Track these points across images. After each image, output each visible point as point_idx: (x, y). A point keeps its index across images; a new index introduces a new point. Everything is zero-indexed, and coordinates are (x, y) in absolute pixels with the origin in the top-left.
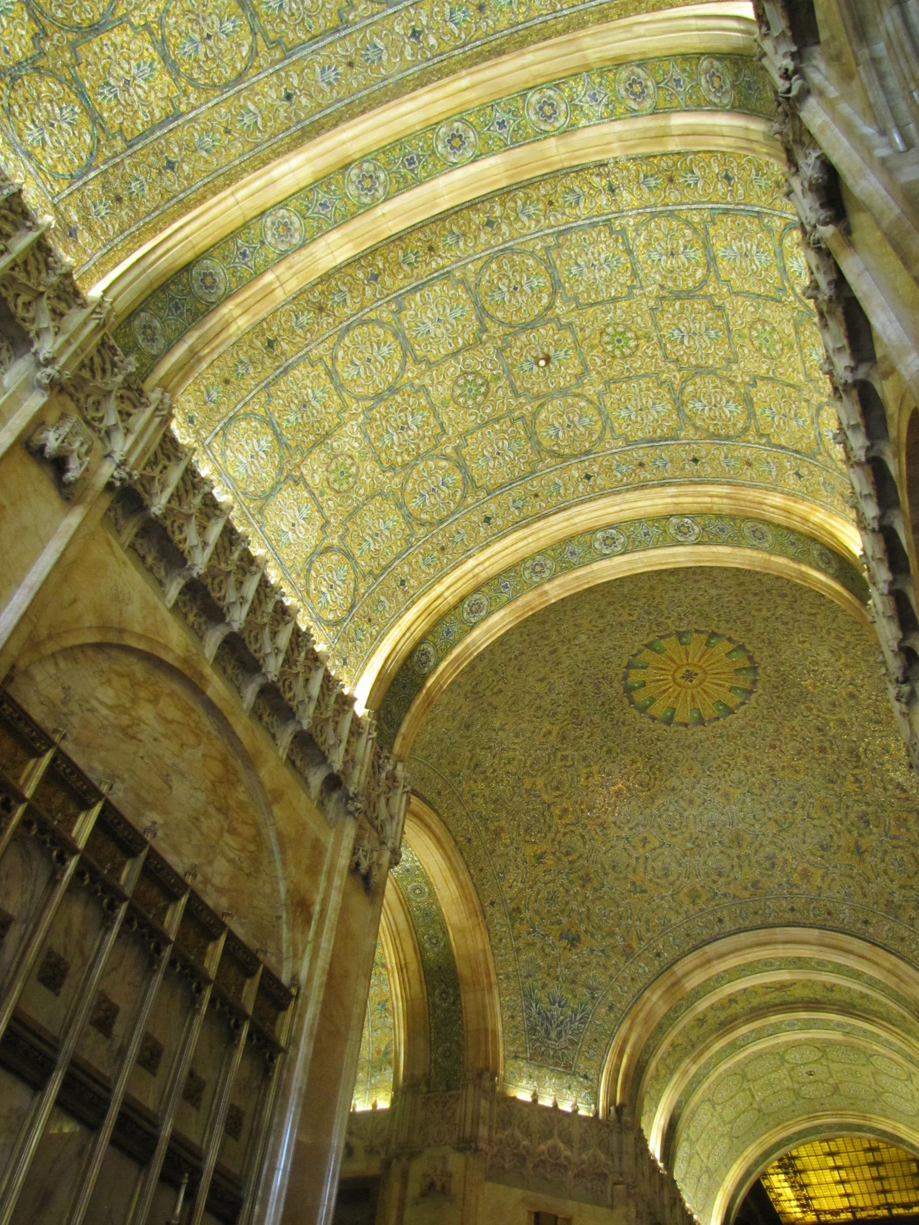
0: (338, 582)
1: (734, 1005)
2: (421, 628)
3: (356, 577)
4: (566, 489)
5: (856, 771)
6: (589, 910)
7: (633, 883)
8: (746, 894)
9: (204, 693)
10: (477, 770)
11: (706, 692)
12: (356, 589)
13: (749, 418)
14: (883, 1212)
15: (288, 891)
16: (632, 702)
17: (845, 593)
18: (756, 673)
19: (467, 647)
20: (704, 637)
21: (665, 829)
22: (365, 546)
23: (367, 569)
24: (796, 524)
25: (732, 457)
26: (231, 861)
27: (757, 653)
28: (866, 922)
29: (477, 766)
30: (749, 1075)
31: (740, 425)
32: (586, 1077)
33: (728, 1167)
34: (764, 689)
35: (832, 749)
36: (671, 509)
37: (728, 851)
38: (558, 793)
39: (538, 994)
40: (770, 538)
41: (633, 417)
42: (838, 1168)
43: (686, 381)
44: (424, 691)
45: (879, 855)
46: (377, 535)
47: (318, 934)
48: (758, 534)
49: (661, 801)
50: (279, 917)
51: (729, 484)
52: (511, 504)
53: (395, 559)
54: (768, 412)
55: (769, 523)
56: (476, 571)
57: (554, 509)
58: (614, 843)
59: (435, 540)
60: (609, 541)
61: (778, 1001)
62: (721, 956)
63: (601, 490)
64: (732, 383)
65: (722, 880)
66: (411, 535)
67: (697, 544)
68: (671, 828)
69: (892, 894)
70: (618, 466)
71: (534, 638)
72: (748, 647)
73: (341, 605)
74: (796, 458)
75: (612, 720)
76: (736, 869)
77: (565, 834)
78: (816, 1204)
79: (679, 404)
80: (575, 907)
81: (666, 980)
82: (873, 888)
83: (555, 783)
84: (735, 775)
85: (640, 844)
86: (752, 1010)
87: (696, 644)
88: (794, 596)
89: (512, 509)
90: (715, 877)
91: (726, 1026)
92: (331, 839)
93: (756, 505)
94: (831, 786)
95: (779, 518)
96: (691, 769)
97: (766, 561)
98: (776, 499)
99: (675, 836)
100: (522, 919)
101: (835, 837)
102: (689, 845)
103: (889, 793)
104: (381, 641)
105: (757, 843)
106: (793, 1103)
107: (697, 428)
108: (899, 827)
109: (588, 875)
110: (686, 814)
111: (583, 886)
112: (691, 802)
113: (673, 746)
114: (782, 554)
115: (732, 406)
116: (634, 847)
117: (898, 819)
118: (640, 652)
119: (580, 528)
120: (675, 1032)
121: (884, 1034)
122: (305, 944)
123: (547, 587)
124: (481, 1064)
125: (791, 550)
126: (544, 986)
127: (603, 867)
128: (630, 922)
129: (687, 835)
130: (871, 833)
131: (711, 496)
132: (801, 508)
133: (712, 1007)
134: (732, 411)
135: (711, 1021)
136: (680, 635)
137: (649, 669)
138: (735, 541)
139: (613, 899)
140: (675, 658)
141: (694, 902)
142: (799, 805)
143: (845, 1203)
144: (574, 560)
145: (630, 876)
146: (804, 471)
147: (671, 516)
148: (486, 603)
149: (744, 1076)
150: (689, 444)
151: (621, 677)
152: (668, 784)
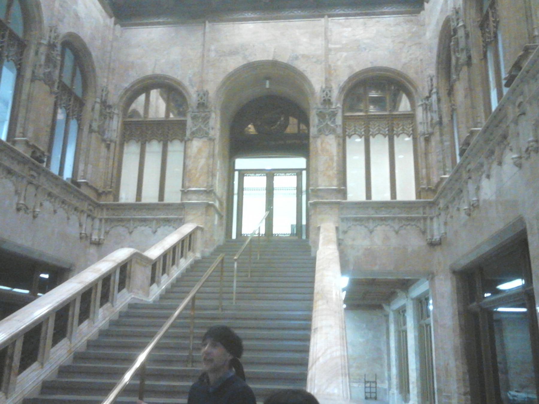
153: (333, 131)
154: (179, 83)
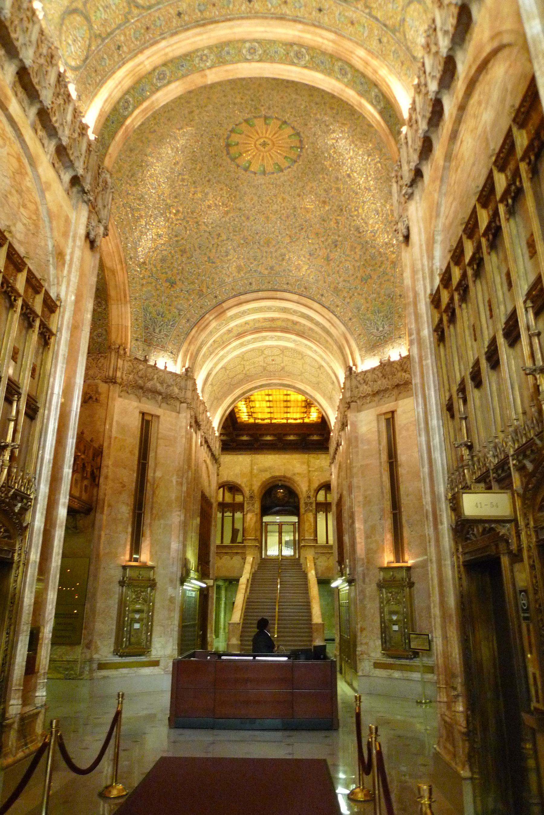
0: (79, 38)
1: (247, 326)
2: (127, 83)
3: (91, 37)
4: (234, 6)
5: (339, 218)
6: (183, 269)
7: (209, 258)
8: (266, 272)
9: (7, 109)
10: (133, 178)
11: (270, 156)
12: (90, 46)
14: (284, 421)
15: (54, 246)
16: (228, 153)
17: (383, 123)
19: (153, 103)
20: (279, 123)
21: (231, 231)
22: (98, 14)
23: (98, 32)
24: (369, 73)
25: (344, 15)
26: (24, 225)
27: (305, 140)
28: (322, 295)
29: (132, 176)
30: (245, 358)
32: (172, 353)
33: (226, 397)
36: (296, 40)
37: (262, 248)
38: (176, 200)
39: (151, 309)
40: (349, 76)
42: (269, 401)
44: (124, 127)
45: (337, 263)
46: (107, 7)
47: (69, 272)
48: (343, 72)
49: (232, 215)
50: (49, 261)
51: (336, 33)
52: (196, 7)
53: (118, 28)
55: (352, 67)
56: (167, 50)
57: (223, 18)
58: (202, 234)
59: (143, 21)
60: (252, 51)
61: (268, 326)
62: (247, 302)
63: (256, 13)
65: (256, 263)
66: (129, 13)
68: (234, 231)
69: (338, 283)
71: (182, 101)
72: (302, 134)
73: (79, 56)
74: (382, 30)
75: (214, 162)
76: (264, 258)
77: (176, 224)
78: (255, 415)
80: (176, 266)
81: (219, 310)
82: (330, 279)
83: (174, 194)
84: (275, 207)
85: (216, 237)
86: (255, 328)
87: (274, 124)
88: (338, 110)
89: (197, 11)
90: (252, 261)
91: (240, 335)
92: (74, 216)
93: (348, 53)
94: (323, 223)
95: (359, 65)
96: (252, 199)
97: (342, 90)
98: (361, 52)
99: (235, 235)
100: (146, 269)
101: (318, 250)
102: (242, 242)
104: (101, 87)
105: (277, 246)
106: (262, 372)
108: (351, 250)
109: (185, 249)
110: (244, 224)
111: (182, 256)
112: (248, 218)
113: (245, 184)
114: (353, 88)
116: (213, 238)
117: (352, 246)
118: (240, 123)
119: (237, 37)
120: (217, 336)
121: (314, 347)
122: (63, 277)
123: (207, 72)
124: (119, 342)
125: (359, 88)
126: (154, 305)
127: (194, 247)
128: (204, 278)
129: (242, 236)
130: (336, 251)
131: (323, 38)
132: (375, 63)
133: (236, 326)
135: (235, 332)
136: (266, 118)
137: (243, 136)
138: (329, 72)
139: (196, 264)
140: (259, 131)
141: (239, 272)
142: (304, 230)
143: (269, 416)
144: (228, 58)
145: (207, 253)
146: (385, 40)
147: (295, 44)
148: (168, 74)
149: (243, 358)
151: (225, 136)
152: (238, 205)
153: (311, 511)
154: (240, 485)
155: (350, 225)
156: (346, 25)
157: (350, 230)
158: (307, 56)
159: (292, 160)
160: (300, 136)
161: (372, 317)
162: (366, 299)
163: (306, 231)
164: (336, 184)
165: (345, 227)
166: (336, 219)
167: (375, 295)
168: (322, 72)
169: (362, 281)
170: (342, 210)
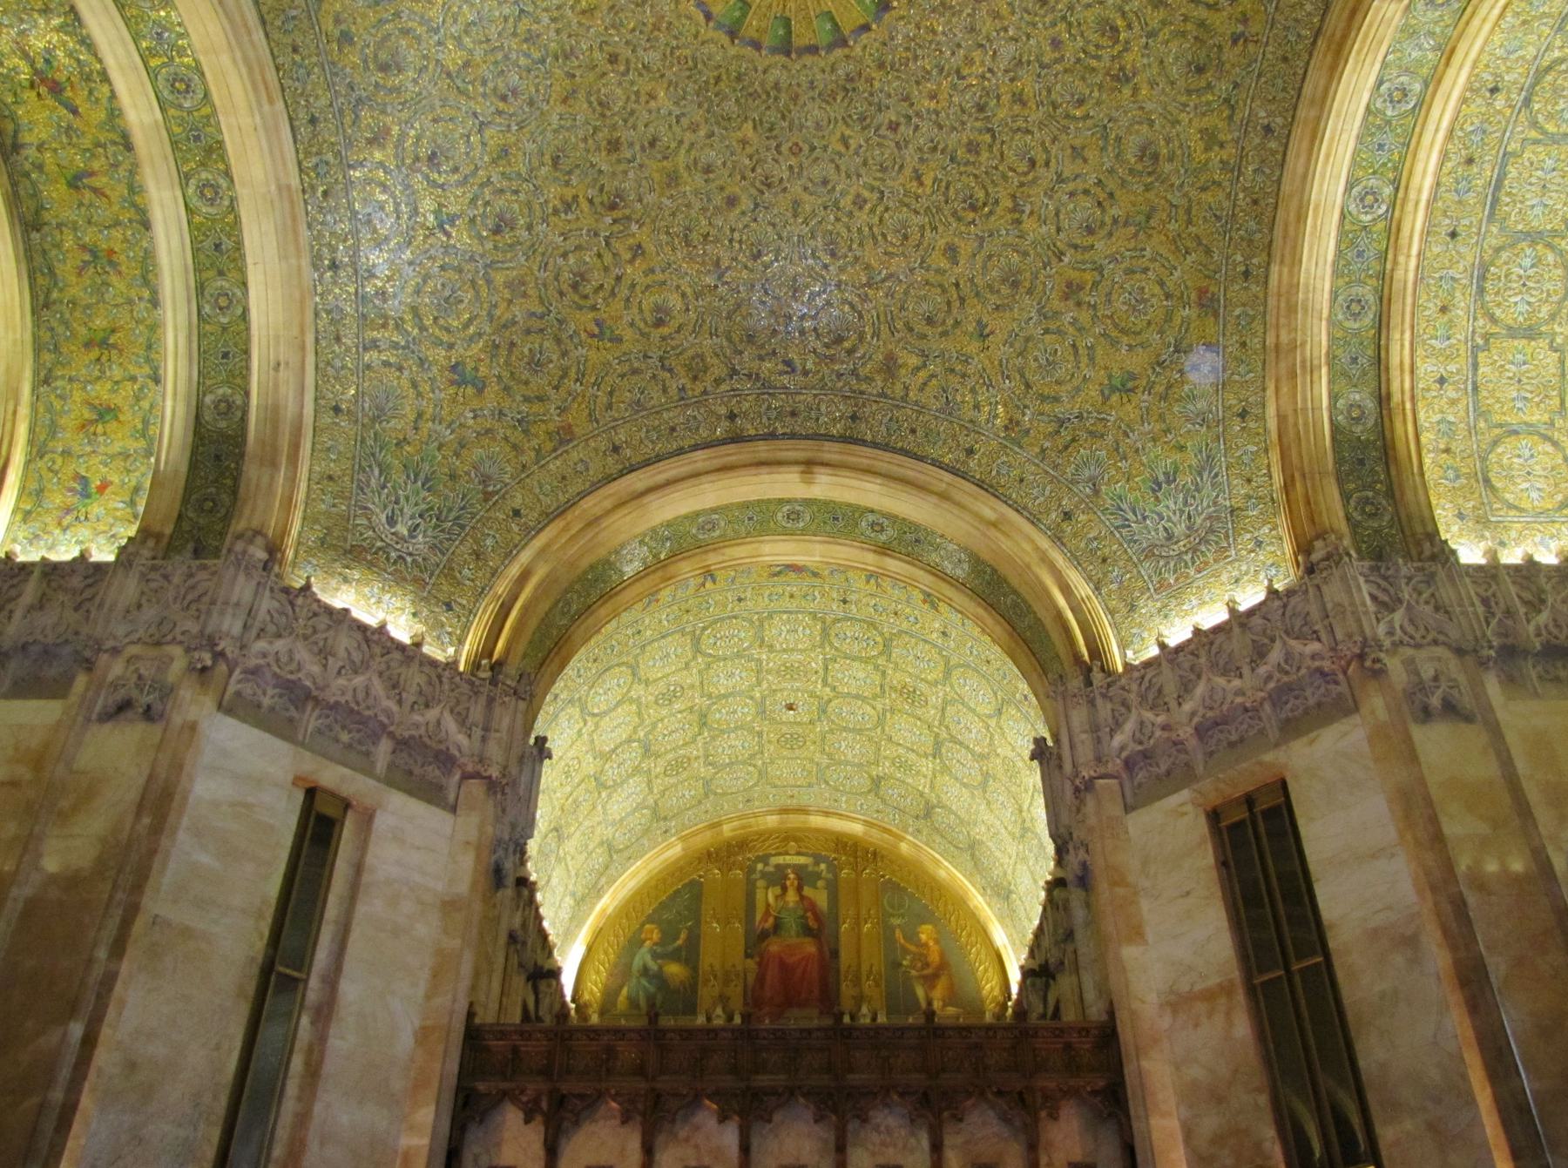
5: (585, 205)
13: (1510, 328)
18: (774, 50)
25: (1454, 289)
31: (1498, 312)
34: (738, 57)
35: (619, 161)
41: (1539, 173)
43: (1561, 256)
48: (1355, 308)
54: (1519, 357)
64: (1553, 317)
67: (1342, 213)
70: (1484, 132)
79: (1533, 237)
94: (547, 159)
103: (560, 261)
107: (1498, 250)
108: (509, 285)
114: (1332, 340)
115: (1523, 308)
130: (481, 238)
134: (1514, 309)
142: (501, 105)
147: (1397, 189)
150: (1478, 234)
155: (578, 248)
156: (1436, 297)
157: (565, 255)
158: (1369, 217)
159: (739, 22)
160: (830, 47)
161: (398, 477)
162: (420, 415)
163: (500, 113)
164: (688, 167)
165: (565, 236)
166: (575, 197)
167: (448, 436)
168: (1339, 253)
169: (453, 368)
170: (613, 207)
